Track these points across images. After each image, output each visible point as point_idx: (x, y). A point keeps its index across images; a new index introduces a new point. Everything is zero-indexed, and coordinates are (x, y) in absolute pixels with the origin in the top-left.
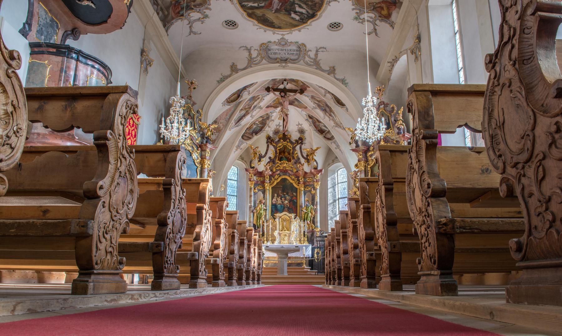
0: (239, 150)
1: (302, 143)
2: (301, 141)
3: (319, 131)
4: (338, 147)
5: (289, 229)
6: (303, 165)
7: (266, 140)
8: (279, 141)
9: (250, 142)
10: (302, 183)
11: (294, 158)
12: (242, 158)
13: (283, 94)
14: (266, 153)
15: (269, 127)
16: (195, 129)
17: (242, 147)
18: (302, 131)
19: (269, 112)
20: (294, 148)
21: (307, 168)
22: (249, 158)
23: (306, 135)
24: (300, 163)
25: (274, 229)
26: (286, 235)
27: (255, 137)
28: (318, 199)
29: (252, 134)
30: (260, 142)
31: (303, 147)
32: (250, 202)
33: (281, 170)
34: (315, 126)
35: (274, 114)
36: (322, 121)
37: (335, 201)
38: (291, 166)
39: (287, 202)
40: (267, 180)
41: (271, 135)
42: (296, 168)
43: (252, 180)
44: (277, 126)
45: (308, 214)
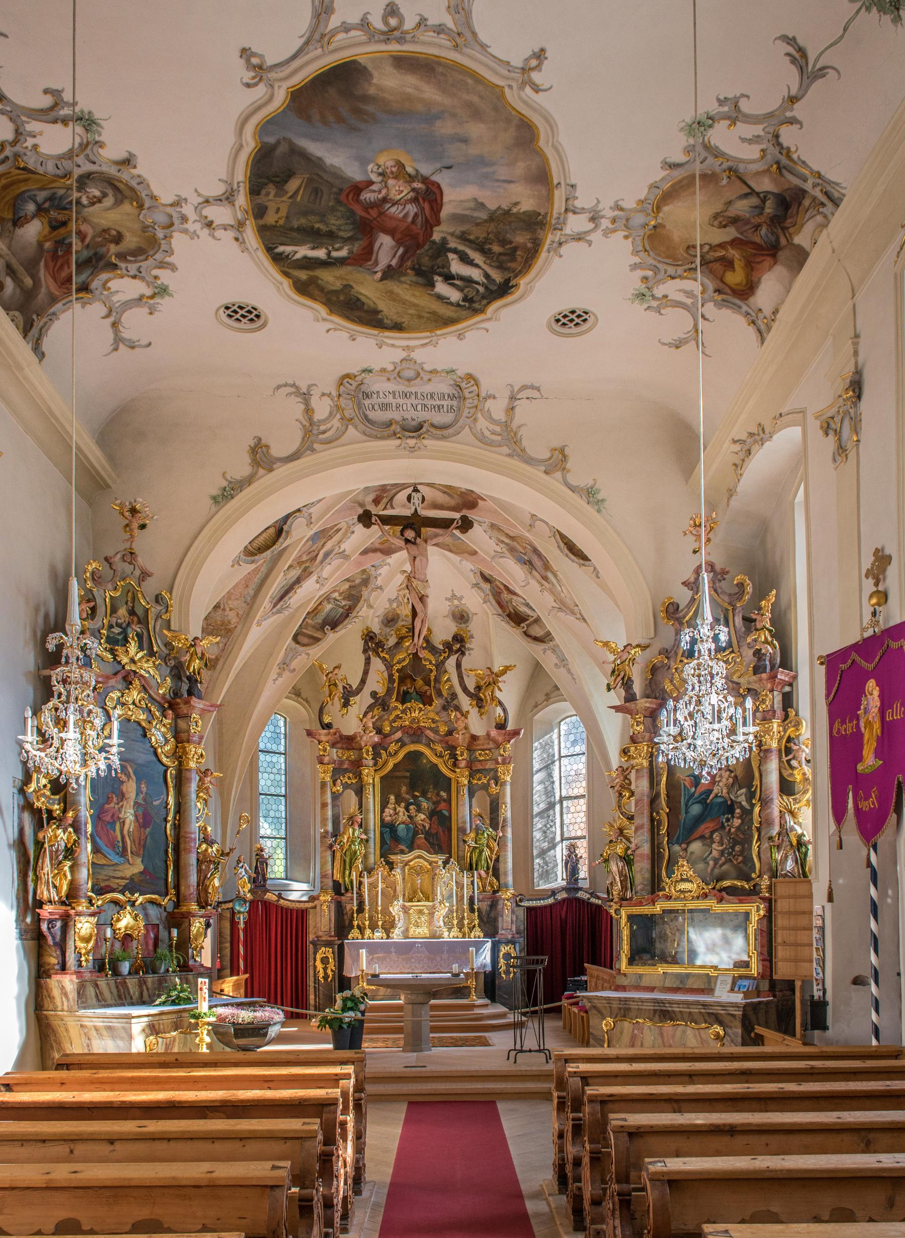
0: (286, 674)
1: (462, 652)
2: (458, 644)
3: (509, 616)
4: (563, 661)
6: (465, 715)
9: (316, 652)
10: (463, 764)
11: (439, 694)
12: (296, 693)
13: (410, 534)
14: (363, 681)
15: (370, 606)
16: (151, 654)
18: (461, 617)
19: (367, 566)
20: (440, 665)
21: (477, 724)
22: (318, 693)
24: (458, 708)
25: (389, 898)
27: (332, 637)
28: (507, 812)
29: (322, 627)
30: (344, 650)
31: (466, 662)
32: (324, 821)
35: (384, 571)
36: (518, 591)
38: (432, 715)
41: (376, 628)
43: (326, 759)
44: (391, 601)
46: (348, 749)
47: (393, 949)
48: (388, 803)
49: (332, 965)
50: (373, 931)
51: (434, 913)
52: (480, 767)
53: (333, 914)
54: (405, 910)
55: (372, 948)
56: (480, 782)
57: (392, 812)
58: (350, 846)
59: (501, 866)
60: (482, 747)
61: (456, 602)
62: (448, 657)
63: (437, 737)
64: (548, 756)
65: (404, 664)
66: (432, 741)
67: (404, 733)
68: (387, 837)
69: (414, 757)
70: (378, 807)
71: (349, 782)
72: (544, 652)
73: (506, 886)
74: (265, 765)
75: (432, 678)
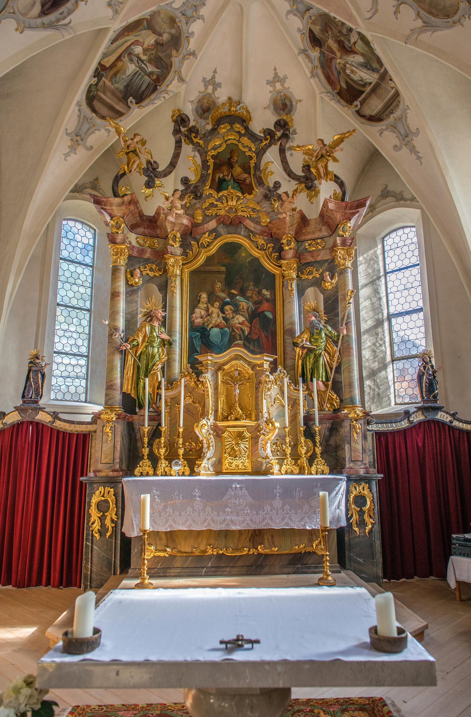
0: (81, 151)
1: (286, 136)
2: (282, 131)
3: (339, 94)
5: (254, 412)
7: (171, 127)
8: (214, 130)
10: (290, 254)
11: (261, 182)
14: (173, 165)
15: (181, 80)
17: (92, 140)
23: (298, 120)
25: (195, 414)
26: (240, 436)
27: (136, 114)
33: (221, 221)
34: (328, 78)
37: (379, 323)
39: (241, 319)
40: (176, 248)
41: (189, 110)
42: (268, 214)
44: (206, 83)
45: (317, 358)
46: (152, 237)
47: (197, 493)
48: (199, 301)
49: (112, 514)
50: (170, 463)
51: (258, 437)
52: (310, 259)
53: (119, 439)
54: (218, 432)
55: (165, 492)
56: (311, 277)
57: (203, 313)
58: (146, 347)
59: (343, 377)
60: (312, 236)
61: (278, 86)
62: (270, 145)
63: (259, 227)
64: (374, 271)
65: (220, 150)
66: (252, 232)
67: (219, 223)
68: (197, 343)
69: (231, 249)
70: (186, 307)
71: (151, 274)
72: (381, 134)
73: (352, 401)
74: (67, 274)
75: (252, 165)
